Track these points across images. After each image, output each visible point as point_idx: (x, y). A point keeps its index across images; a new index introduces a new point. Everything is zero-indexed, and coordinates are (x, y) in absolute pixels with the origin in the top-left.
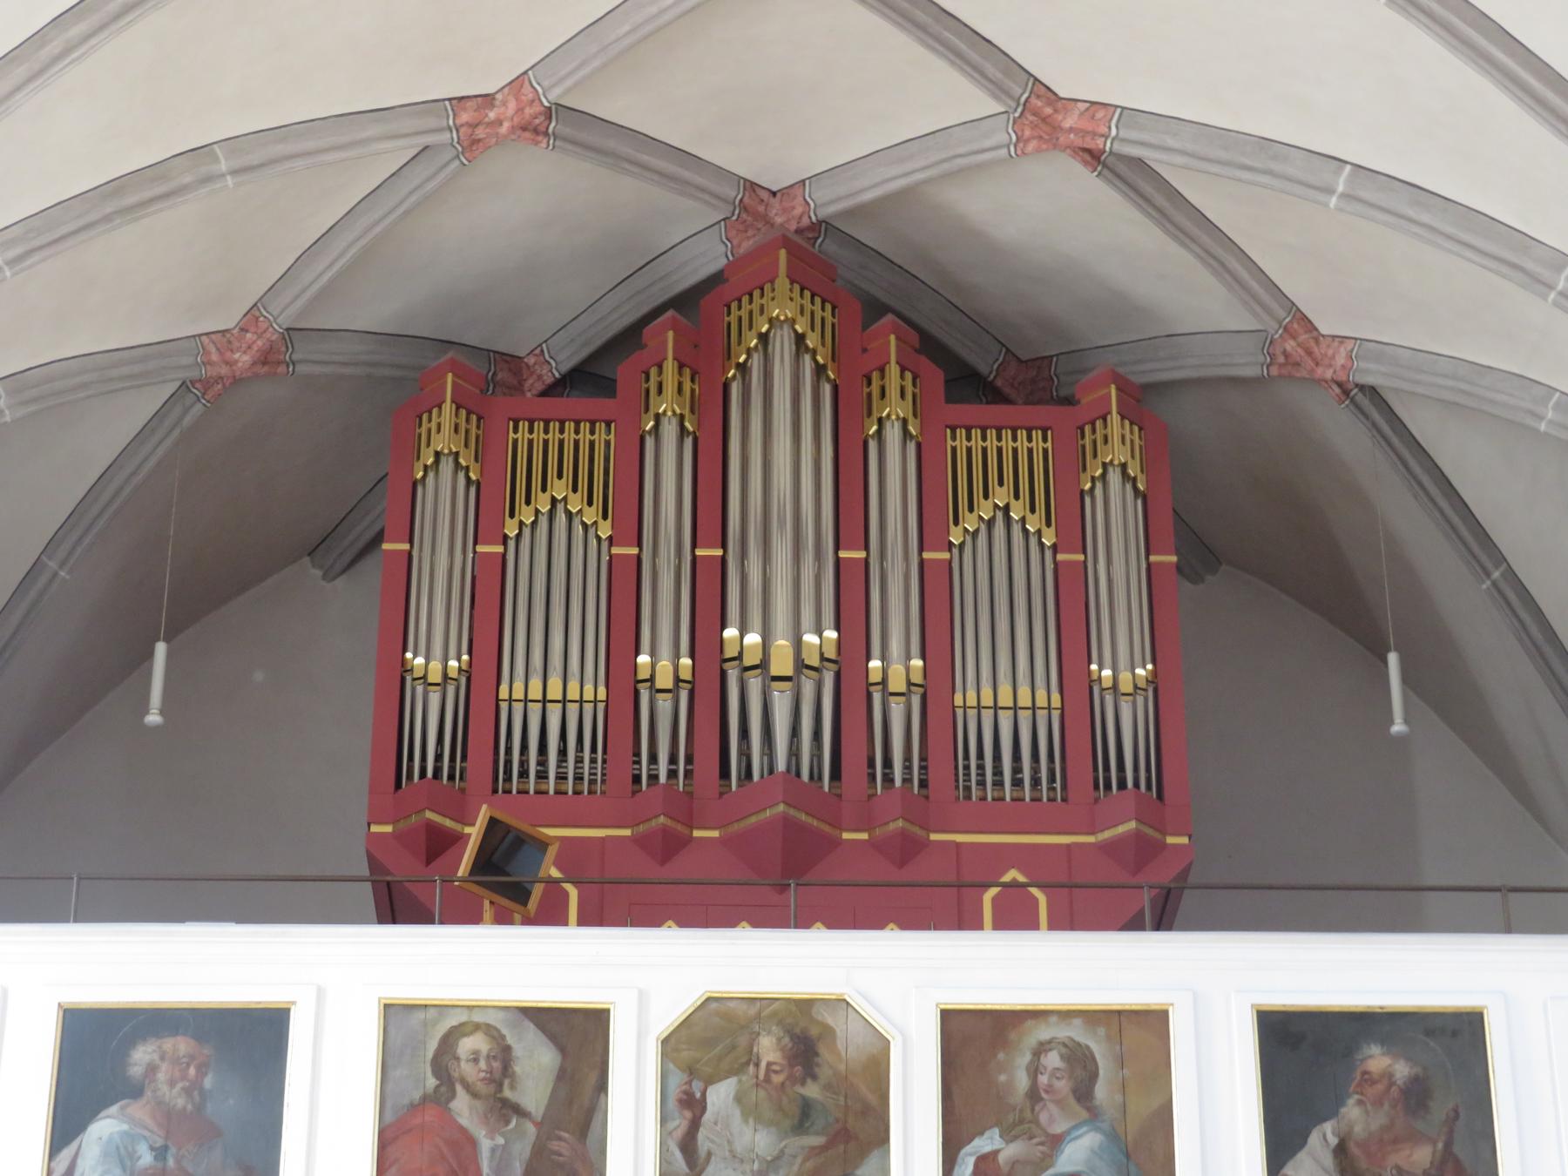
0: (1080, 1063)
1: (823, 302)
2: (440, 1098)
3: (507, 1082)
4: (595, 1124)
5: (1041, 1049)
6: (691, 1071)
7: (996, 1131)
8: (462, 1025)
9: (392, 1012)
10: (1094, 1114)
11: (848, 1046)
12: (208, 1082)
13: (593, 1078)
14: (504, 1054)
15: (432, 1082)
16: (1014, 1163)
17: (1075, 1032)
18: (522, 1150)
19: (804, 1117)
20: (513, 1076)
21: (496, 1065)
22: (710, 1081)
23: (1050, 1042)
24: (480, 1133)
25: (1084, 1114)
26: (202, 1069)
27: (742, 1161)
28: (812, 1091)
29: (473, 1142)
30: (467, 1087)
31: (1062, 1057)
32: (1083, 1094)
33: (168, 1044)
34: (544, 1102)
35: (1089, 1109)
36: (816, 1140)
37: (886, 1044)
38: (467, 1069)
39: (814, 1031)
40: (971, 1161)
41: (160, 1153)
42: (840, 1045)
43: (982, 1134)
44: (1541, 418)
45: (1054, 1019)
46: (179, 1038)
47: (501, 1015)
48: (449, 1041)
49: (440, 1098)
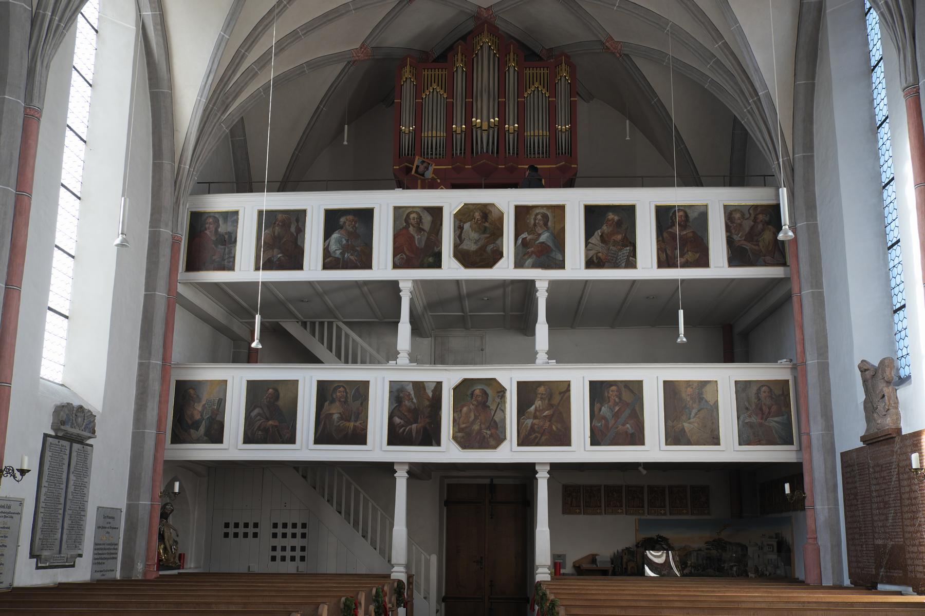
0: (545, 217)
1: (493, 35)
2: (406, 228)
3: (421, 224)
4: (440, 233)
5: (537, 214)
6: (461, 221)
7: (526, 233)
8: (411, 211)
9: (396, 209)
10: (548, 229)
11: (495, 215)
12: (357, 225)
13: (439, 223)
14: (420, 218)
15: (405, 224)
16: (530, 240)
17: (544, 211)
18: (424, 239)
19: (485, 230)
20: (422, 223)
21: (419, 220)
22: (464, 223)
23: (539, 213)
24: (415, 235)
25: (546, 229)
26: (355, 223)
27: (471, 240)
28: (487, 224)
29: (414, 237)
30: (413, 225)
31: (542, 216)
32: (546, 224)
33: (348, 217)
34: (429, 227)
35: (547, 228)
36: (488, 235)
37: (503, 214)
38: (412, 221)
39: (487, 211)
40: (521, 239)
41: (347, 241)
42: (493, 215)
43: (523, 233)
44: (664, 62)
45: (540, 208)
46: (350, 216)
47: (419, 209)
48: (408, 215)
49: (406, 228)
